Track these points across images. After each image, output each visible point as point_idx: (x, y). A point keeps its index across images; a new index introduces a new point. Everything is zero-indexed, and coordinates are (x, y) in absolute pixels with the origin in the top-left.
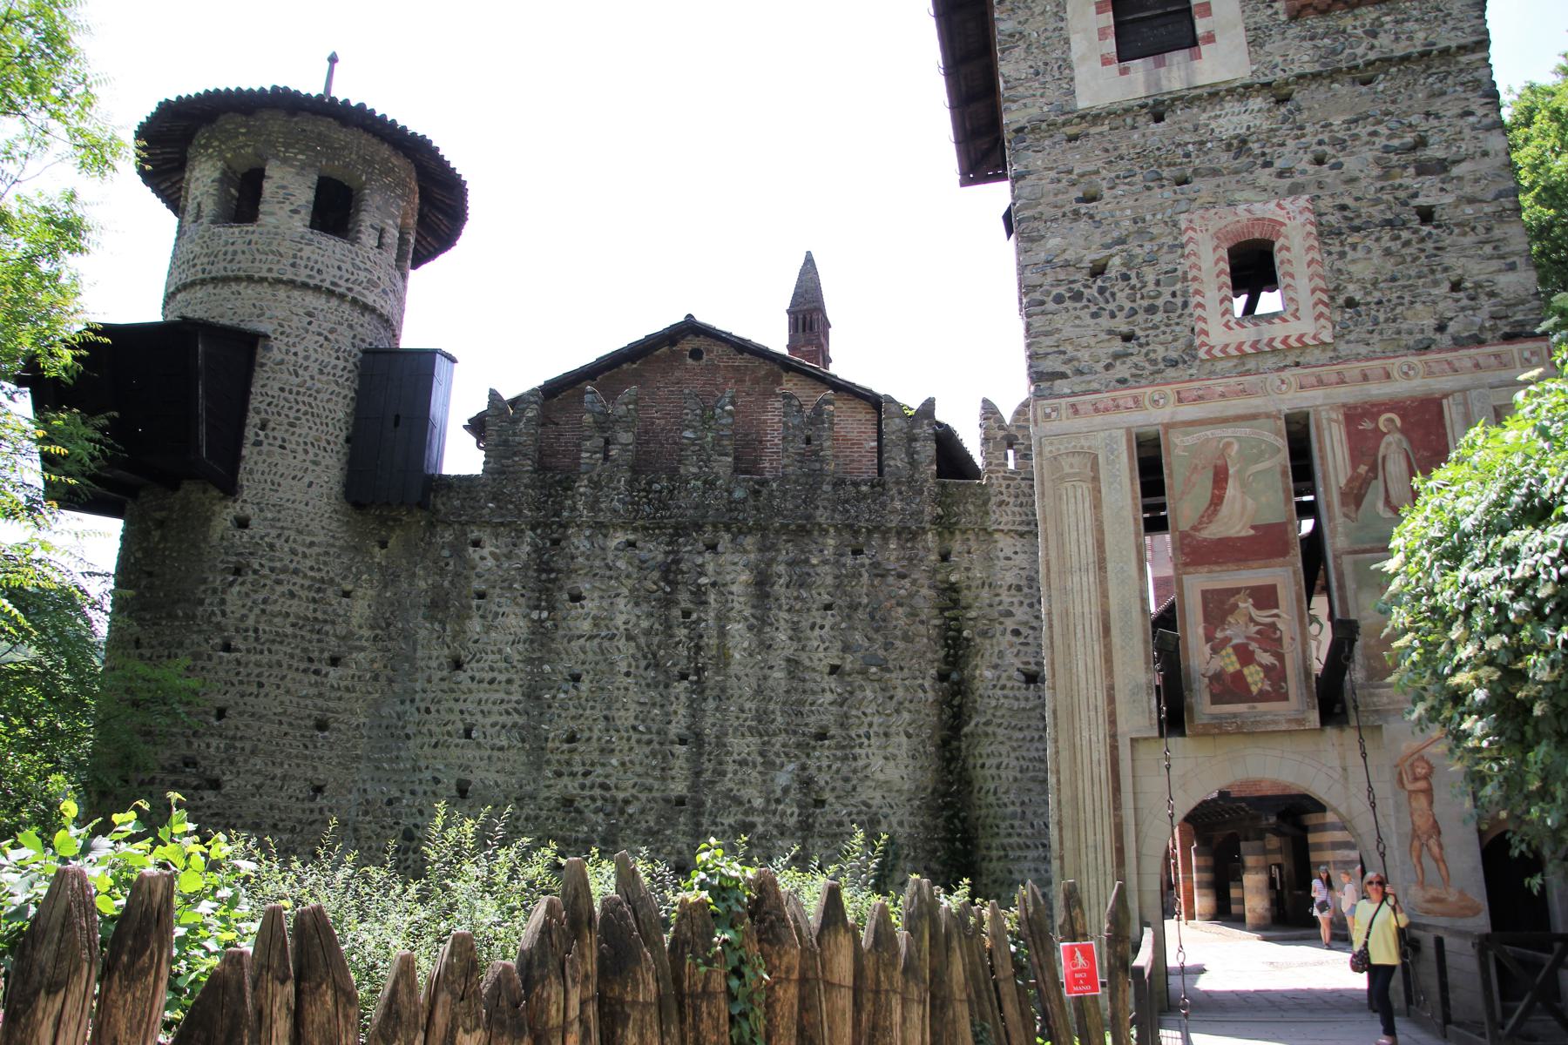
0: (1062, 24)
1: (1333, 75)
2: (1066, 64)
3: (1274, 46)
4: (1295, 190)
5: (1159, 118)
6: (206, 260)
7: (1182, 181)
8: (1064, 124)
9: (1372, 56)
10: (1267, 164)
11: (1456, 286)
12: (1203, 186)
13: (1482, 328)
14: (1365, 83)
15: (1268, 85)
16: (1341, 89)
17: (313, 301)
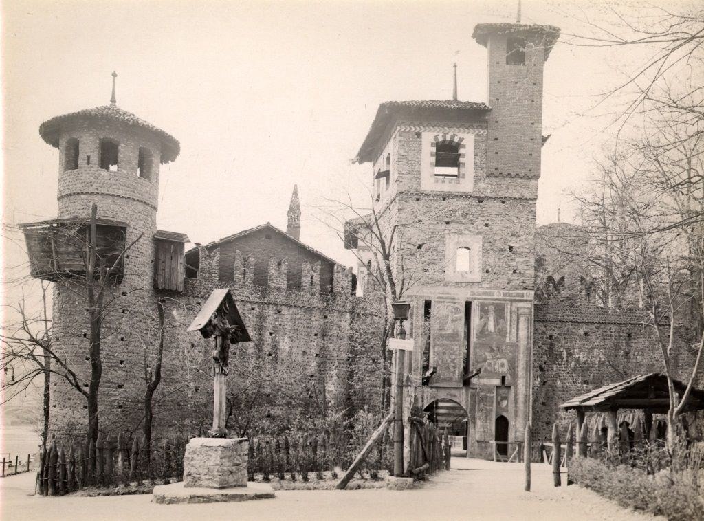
0: (419, 157)
1: (495, 198)
2: (419, 173)
3: (482, 185)
4: (479, 233)
5: (444, 199)
6: (98, 185)
7: (447, 223)
8: (417, 194)
9: (507, 195)
10: (473, 224)
11: (515, 272)
12: (453, 226)
13: (519, 285)
14: (503, 202)
15: (477, 197)
16: (497, 203)
17: (140, 207)
